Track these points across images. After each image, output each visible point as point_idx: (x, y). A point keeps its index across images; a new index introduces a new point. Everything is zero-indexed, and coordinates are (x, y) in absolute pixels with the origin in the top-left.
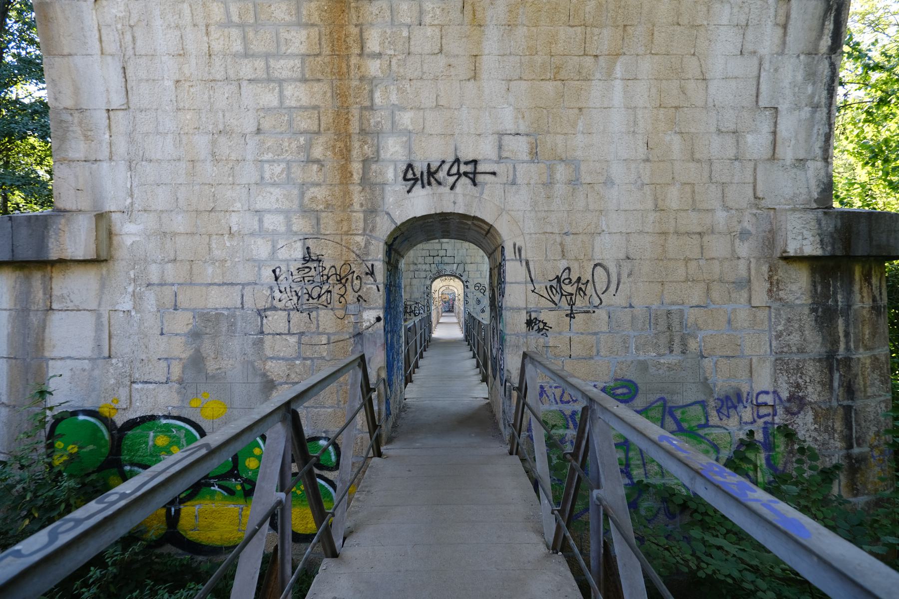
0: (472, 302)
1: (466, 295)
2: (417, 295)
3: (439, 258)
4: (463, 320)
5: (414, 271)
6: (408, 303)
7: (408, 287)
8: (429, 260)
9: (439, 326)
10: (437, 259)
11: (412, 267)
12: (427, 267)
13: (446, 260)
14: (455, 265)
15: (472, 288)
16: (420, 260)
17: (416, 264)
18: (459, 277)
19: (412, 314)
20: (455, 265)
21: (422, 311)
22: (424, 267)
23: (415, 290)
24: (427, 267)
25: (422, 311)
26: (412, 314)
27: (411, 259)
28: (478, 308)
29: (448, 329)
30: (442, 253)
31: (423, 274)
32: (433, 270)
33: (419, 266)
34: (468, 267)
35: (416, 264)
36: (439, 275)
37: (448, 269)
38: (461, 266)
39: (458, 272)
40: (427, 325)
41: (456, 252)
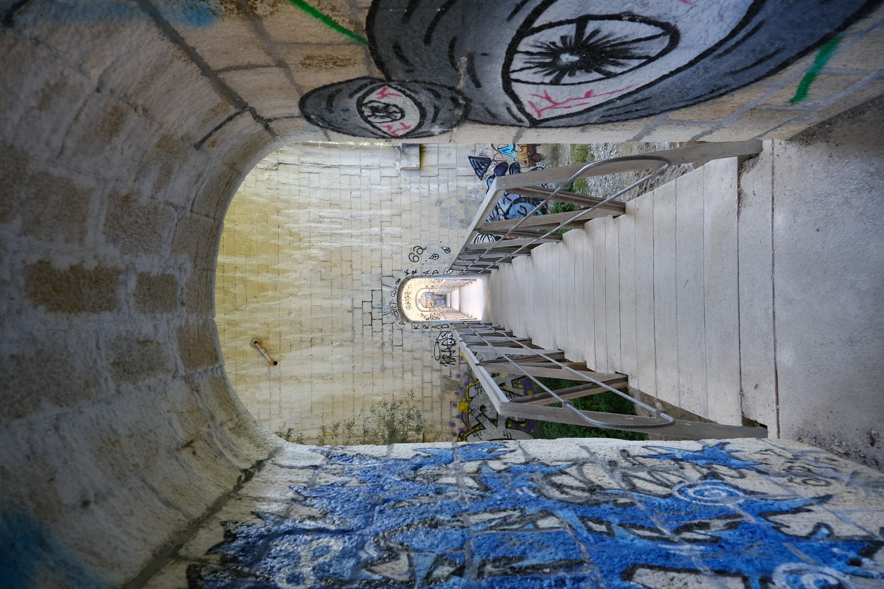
0: (435, 265)
1: (426, 275)
2: (426, 342)
3: (375, 312)
4: (459, 280)
5: (393, 346)
6: (437, 354)
7: (416, 355)
8: (377, 325)
9: (464, 310)
10: (376, 314)
11: (388, 349)
12: (387, 328)
13: (377, 302)
14: (385, 289)
15: (415, 266)
16: (377, 338)
17: (383, 344)
18: (402, 284)
19: (453, 348)
20: (385, 289)
21: (449, 335)
22: (387, 332)
23: (419, 345)
24: (387, 328)
25: (449, 335)
26: (453, 348)
27: (377, 350)
28: (444, 256)
29: (472, 300)
30: (367, 306)
31: (397, 334)
32: (391, 320)
33: (386, 339)
34: (387, 271)
35: (383, 344)
36: (398, 311)
37: (389, 299)
38: (386, 281)
39: (394, 285)
40: (467, 326)
41: (366, 288)
